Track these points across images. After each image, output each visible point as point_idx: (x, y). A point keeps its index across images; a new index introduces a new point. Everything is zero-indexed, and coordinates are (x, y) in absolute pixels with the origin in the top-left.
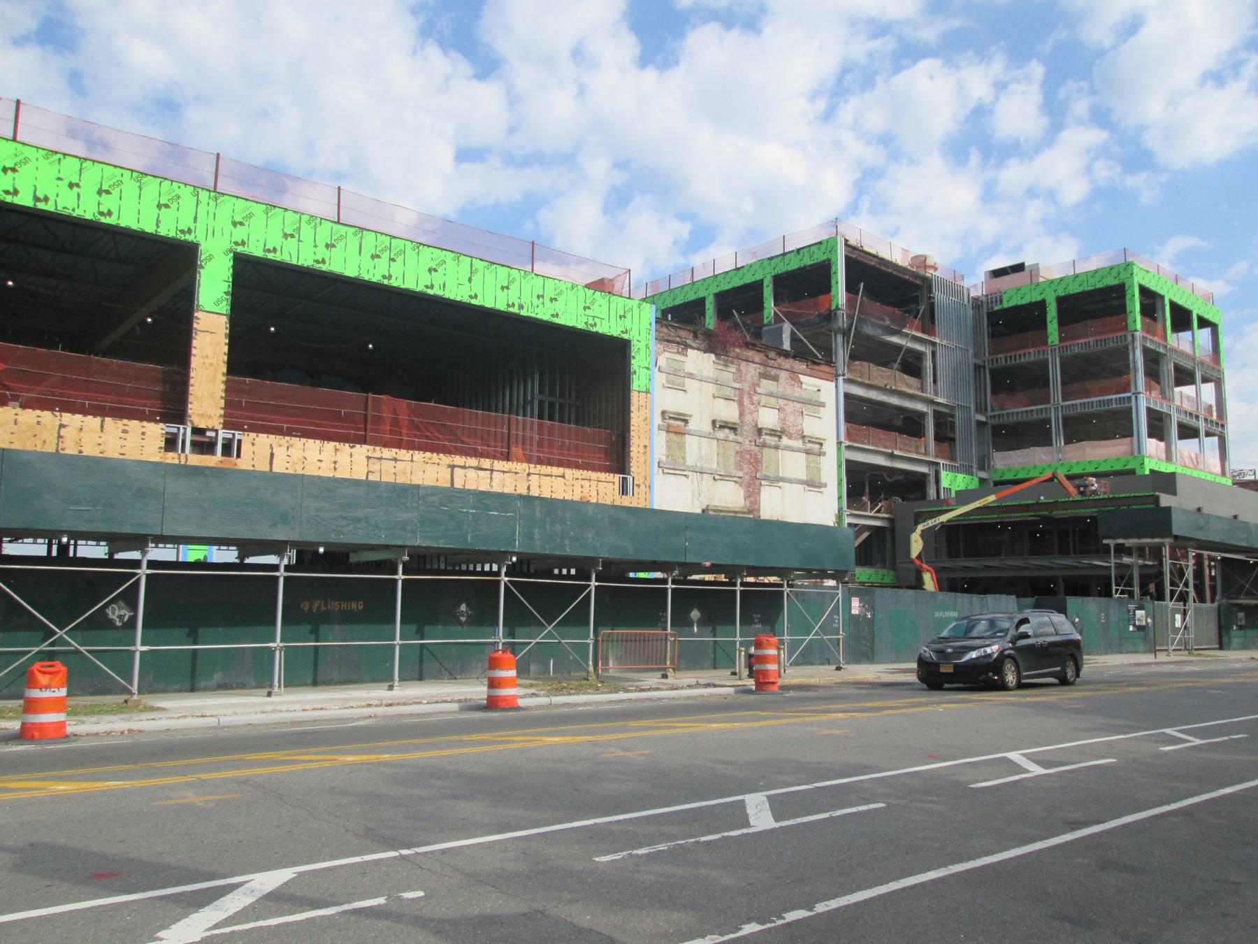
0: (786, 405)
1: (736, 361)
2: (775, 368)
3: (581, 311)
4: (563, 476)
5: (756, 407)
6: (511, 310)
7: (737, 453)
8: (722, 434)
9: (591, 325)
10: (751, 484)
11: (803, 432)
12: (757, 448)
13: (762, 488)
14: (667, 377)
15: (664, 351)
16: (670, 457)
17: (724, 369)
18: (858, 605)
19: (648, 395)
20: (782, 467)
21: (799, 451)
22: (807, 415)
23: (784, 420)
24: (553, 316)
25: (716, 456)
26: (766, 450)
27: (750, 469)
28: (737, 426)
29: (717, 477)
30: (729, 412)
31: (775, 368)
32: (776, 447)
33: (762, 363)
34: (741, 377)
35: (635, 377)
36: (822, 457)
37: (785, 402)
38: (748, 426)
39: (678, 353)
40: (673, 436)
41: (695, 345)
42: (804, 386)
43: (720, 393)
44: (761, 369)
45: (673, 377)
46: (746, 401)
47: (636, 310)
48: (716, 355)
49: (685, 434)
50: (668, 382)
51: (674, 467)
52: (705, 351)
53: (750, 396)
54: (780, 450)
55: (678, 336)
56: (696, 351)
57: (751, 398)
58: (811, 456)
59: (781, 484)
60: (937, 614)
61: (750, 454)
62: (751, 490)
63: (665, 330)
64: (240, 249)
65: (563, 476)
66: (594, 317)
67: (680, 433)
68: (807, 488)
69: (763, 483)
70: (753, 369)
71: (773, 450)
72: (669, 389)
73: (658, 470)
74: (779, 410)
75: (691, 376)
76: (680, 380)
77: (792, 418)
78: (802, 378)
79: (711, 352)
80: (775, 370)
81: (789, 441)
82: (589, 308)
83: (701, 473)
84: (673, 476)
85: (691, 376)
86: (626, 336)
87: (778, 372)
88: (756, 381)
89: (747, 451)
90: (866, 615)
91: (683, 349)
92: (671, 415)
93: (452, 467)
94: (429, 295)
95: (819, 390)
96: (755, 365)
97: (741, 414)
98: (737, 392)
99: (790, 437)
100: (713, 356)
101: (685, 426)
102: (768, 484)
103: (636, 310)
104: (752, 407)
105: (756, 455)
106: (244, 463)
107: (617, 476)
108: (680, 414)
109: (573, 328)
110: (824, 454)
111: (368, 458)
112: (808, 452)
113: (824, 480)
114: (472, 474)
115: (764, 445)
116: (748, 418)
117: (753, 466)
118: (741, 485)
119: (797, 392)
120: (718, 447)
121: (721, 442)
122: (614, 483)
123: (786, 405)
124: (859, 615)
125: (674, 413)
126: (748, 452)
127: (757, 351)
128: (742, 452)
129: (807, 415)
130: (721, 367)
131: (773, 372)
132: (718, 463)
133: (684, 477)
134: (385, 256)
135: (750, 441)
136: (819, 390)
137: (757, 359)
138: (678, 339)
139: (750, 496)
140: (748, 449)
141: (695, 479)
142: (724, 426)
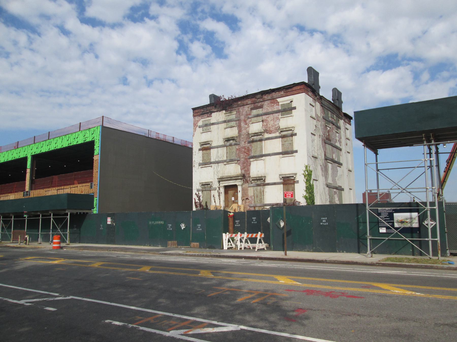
0: (268, 117)
1: (237, 109)
2: (262, 101)
3: (83, 137)
4: (77, 187)
5: (248, 125)
6: (69, 145)
7: (237, 149)
8: (228, 144)
9: (85, 141)
10: (245, 162)
11: (280, 127)
12: (249, 144)
13: (251, 163)
14: (202, 129)
15: (201, 119)
16: (204, 161)
17: (230, 114)
18: (110, 220)
19: (99, 155)
20: (264, 149)
21: (276, 138)
22: (281, 118)
23: (267, 125)
24: (77, 142)
25: (226, 154)
26: (254, 144)
27: (245, 155)
28: (234, 138)
29: (225, 163)
30: (233, 132)
31: (262, 101)
32: (261, 140)
33: (253, 102)
34: (240, 114)
35: (95, 151)
36: (293, 137)
37: (267, 116)
38: (244, 135)
39: (208, 117)
40: (204, 151)
41: (215, 110)
42: (280, 104)
43: (228, 126)
44: (252, 106)
45: (205, 128)
46: (243, 124)
47: (96, 130)
48: (226, 110)
49: (210, 149)
50: (203, 130)
51: (206, 163)
52: (220, 111)
53: (245, 121)
54: (263, 141)
55: (208, 110)
56: (216, 113)
57: (245, 122)
58: (285, 139)
59: (264, 158)
60: (150, 223)
61: (245, 148)
62: (245, 165)
63: (202, 110)
64: (32, 154)
65: (77, 187)
66: (86, 138)
67: (208, 149)
68: (281, 156)
69: (252, 160)
70: (247, 108)
71: (259, 143)
72: (203, 133)
73: (199, 167)
74: (263, 121)
75: (213, 124)
76: (209, 127)
77: (272, 122)
78: (279, 100)
79: (223, 110)
80: (260, 103)
81: (270, 135)
82: (85, 136)
83: (217, 163)
84: (205, 168)
85: (213, 124)
86: (93, 139)
87: (263, 103)
88: (248, 112)
89: (243, 147)
90: (113, 224)
91: (210, 114)
92: (202, 144)
93: (57, 190)
94: (78, 144)
95: (291, 102)
96: (248, 106)
97: (240, 131)
98: (237, 122)
99: (270, 132)
100: (224, 112)
101: (211, 146)
102: (254, 160)
103: (96, 130)
104: (246, 126)
105: (248, 148)
106: (31, 196)
107: (90, 183)
108: (205, 142)
109: (81, 143)
110: (295, 134)
111: (45, 191)
112: (283, 137)
113: (295, 149)
114: (60, 190)
115: (253, 141)
116: (244, 132)
117: (247, 153)
118: (239, 164)
119: (276, 108)
120: (227, 150)
121: (228, 147)
122: (89, 186)
123: (268, 117)
124: (111, 224)
125: (203, 142)
126: (244, 148)
127: (251, 98)
128: (240, 148)
129: (281, 118)
130: (228, 114)
131: (259, 105)
132: (227, 157)
133: (210, 167)
134: (49, 145)
135: (245, 142)
136: (291, 102)
137: (249, 102)
138: (208, 111)
139: (245, 168)
140: (243, 146)
141: (215, 167)
142: (228, 140)
